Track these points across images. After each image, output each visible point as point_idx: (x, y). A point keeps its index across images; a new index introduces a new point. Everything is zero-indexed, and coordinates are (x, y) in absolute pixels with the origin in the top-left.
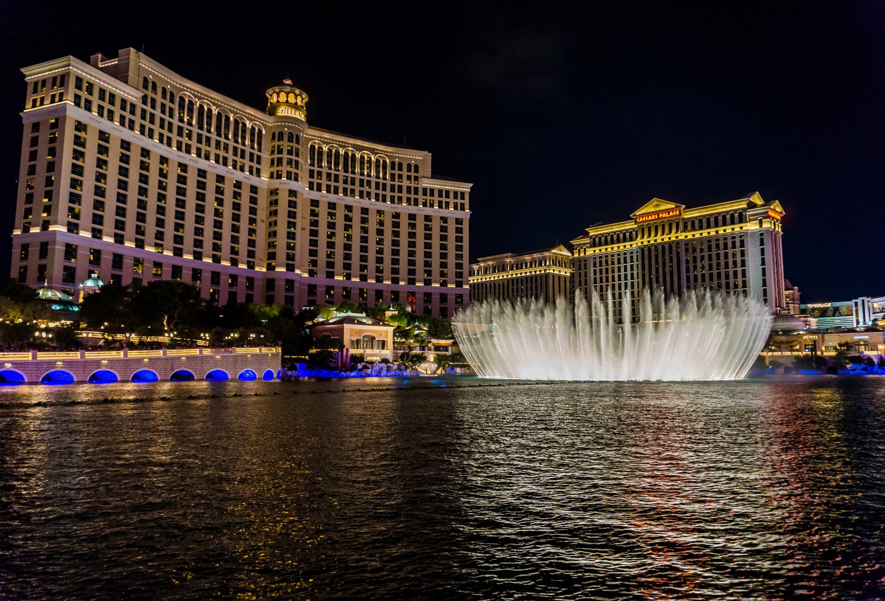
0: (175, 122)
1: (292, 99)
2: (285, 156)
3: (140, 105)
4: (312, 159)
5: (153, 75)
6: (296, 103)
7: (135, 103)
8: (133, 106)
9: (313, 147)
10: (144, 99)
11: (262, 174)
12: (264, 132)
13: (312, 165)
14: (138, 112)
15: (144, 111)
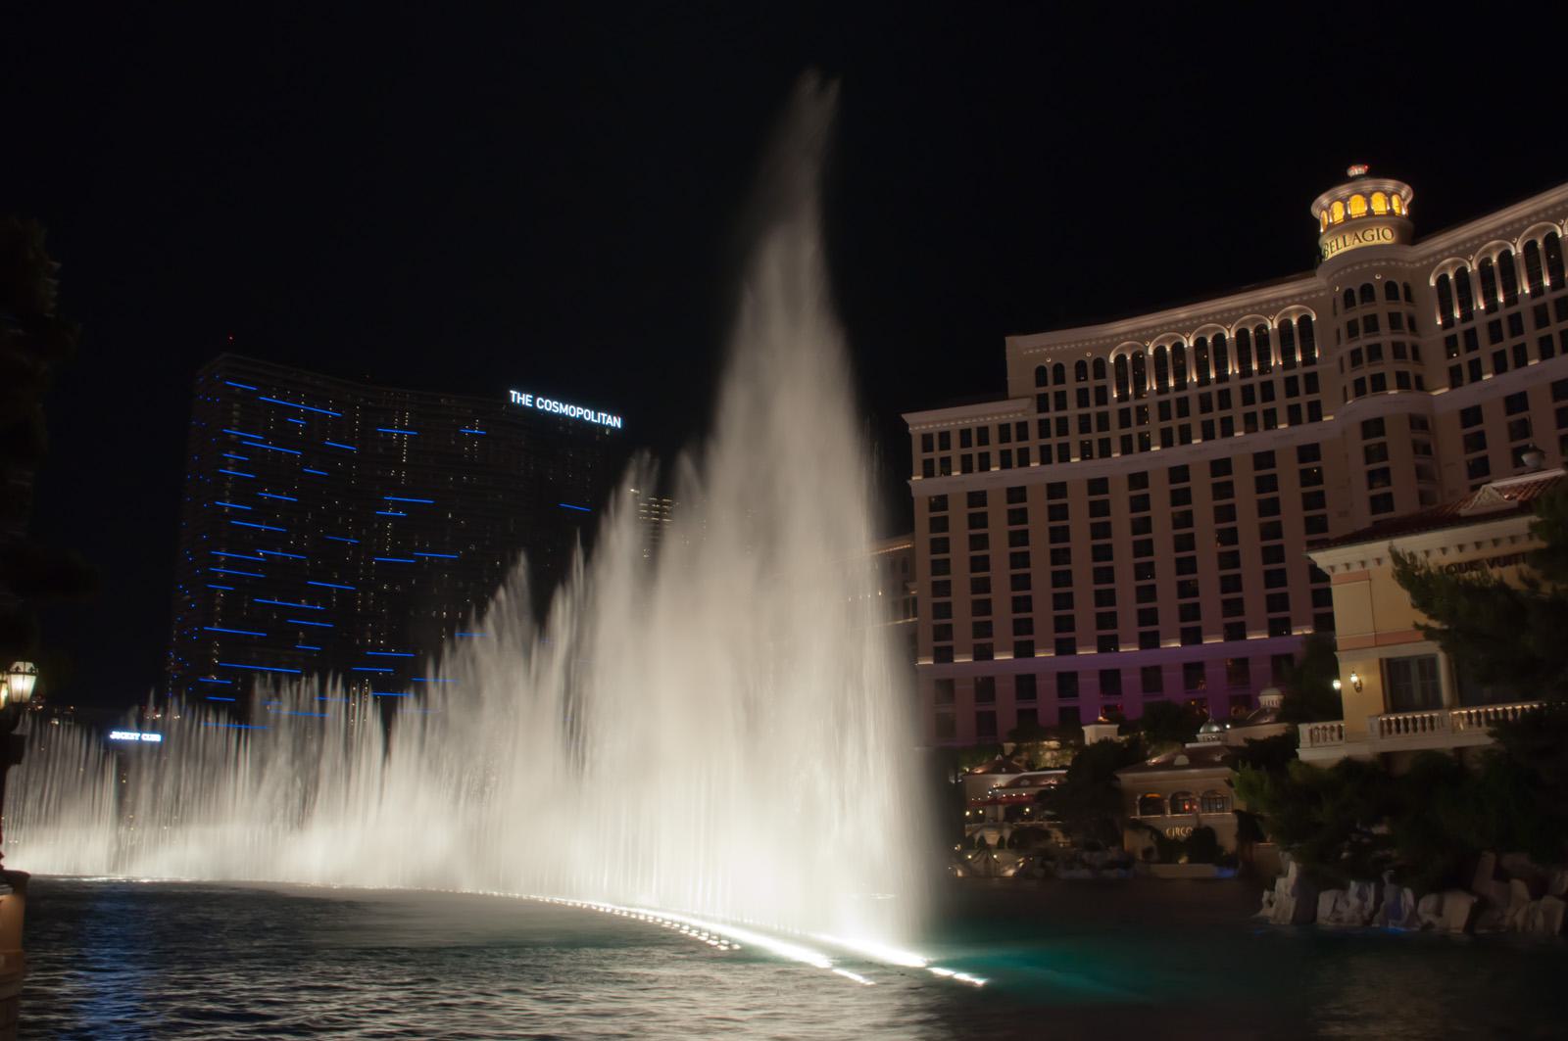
0: (1113, 408)
1: (1338, 213)
2: (1385, 337)
3: (1033, 417)
4: (1446, 312)
5: (1048, 354)
6: (1347, 218)
7: (1023, 419)
8: (1022, 427)
9: (1443, 280)
10: (1042, 404)
11: (1324, 409)
12: (1314, 319)
13: (1449, 322)
14: (1033, 430)
15: (1044, 428)
